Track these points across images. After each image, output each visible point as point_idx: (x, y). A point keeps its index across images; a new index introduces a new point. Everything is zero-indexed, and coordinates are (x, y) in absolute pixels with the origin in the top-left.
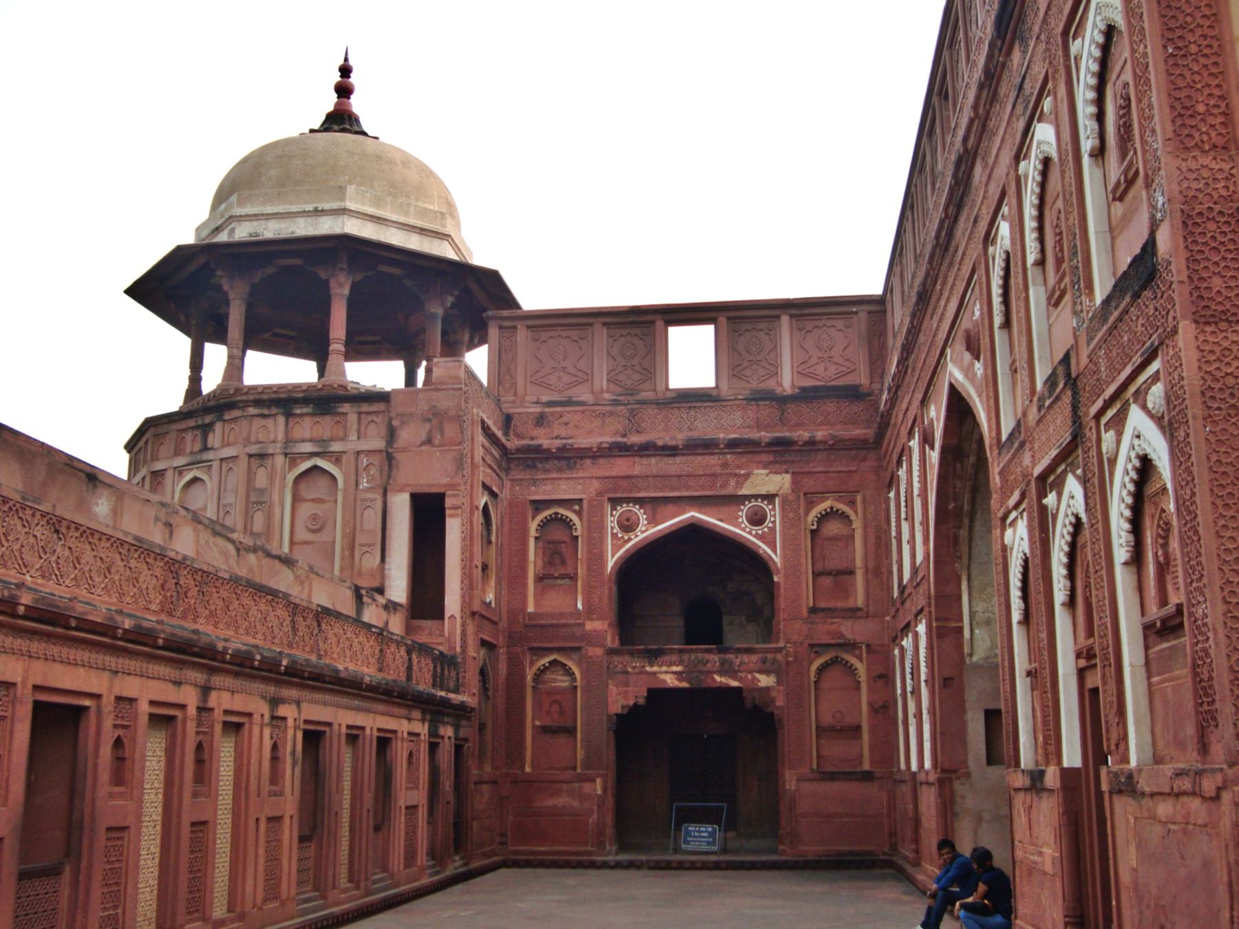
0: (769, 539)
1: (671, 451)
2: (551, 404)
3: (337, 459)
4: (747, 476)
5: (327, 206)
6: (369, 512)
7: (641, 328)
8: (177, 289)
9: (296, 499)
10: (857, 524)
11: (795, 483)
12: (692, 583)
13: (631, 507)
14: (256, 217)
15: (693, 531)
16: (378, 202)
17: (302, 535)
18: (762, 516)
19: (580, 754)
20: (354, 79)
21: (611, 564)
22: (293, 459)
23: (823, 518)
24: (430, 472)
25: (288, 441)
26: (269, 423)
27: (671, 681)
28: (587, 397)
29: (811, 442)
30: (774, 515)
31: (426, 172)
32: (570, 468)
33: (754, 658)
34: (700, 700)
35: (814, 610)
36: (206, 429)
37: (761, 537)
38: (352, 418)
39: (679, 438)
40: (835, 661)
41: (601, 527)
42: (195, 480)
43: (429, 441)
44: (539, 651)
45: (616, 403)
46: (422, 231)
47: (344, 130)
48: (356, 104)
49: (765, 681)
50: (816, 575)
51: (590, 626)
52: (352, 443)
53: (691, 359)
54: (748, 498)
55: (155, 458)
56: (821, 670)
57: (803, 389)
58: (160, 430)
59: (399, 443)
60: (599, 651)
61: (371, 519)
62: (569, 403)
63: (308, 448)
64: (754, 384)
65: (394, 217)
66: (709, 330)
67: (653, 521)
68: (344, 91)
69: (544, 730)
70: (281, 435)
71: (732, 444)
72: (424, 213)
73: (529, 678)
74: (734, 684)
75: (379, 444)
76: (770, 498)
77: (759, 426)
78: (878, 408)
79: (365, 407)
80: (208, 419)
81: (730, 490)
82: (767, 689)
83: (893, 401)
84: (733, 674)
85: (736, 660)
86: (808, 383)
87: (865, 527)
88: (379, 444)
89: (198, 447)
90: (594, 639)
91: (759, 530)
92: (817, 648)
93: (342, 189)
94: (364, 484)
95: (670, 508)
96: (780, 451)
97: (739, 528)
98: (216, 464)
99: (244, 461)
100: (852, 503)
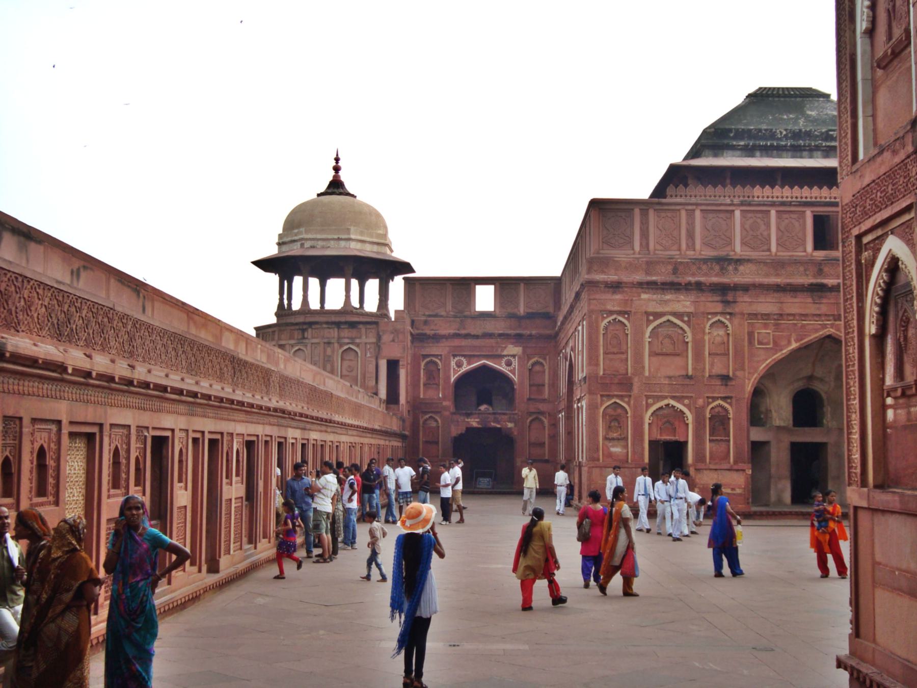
0: (513, 372)
1: (476, 337)
2: (430, 316)
3: (358, 345)
4: (505, 347)
5: (343, 237)
6: (370, 366)
7: (465, 286)
8: (280, 266)
9: (342, 359)
10: (546, 367)
11: (524, 352)
12: (484, 386)
13: (462, 359)
15: (484, 367)
16: (362, 233)
17: (345, 373)
18: (510, 363)
19: (440, 452)
20: (340, 164)
21: (452, 380)
22: (341, 345)
23: (533, 365)
24: (395, 352)
25: (339, 338)
26: (331, 330)
27: (475, 424)
28: (443, 313)
29: (530, 335)
30: (515, 363)
31: (378, 215)
32: (438, 342)
33: (506, 417)
34: (486, 431)
35: (529, 399)
36: (304, 331)
37: (510, 371)
38: (363, 330)
39: (479, 332)
40: (537, 418)
41: (450, 364)
42: (299, 349)
43: (393, 341)
44: (425, 413)
45: (455, 317)
46: (378, 244)
47: (340, 194)
48: (343, 176)
49: (510, 425)
50: (530, 386)
51: (445, 403)
52: (364, 339)
53: (485, 299)
54: (506, 356)
55: (279, 339)
56: (531, 422)
57: (528, 313)
58: (282, 328)
59: (383, 341)
60: (447, 413)
61: (372, 368)
62: (436, 316)
63: (346, 341)
64: (509, 310)
65: (368, 239)
66: (491, 288)
67: (469, 364)
68: (337, 169)
69: (427, 442)
70: (336, 335)
71: (500, 335)
72: (379, 236)
73: (421, 423)
74: (499, 426)
75: (374, 340)
76: (514, 356)
77: (511, 329)
78: (556, 323)
79: (368, 326)
80: (305, 327)
81: (499, 352)
82: (510, 428)
83: (560, 329)
84: (498, 422)
85: (500, 417)
86: (530, 311)
87: (550, 368)
88: (374, 340)
89: (300, 337)
90: (446, 408)
91: (509, 368)
92: (530, 414)
93: (348, 231)
94: (368, 355)
95: (475, 359)
96: (518, 339)
97: (502, 367)
98: (309, 346)
99: (322, 345)
100: (545, 359)
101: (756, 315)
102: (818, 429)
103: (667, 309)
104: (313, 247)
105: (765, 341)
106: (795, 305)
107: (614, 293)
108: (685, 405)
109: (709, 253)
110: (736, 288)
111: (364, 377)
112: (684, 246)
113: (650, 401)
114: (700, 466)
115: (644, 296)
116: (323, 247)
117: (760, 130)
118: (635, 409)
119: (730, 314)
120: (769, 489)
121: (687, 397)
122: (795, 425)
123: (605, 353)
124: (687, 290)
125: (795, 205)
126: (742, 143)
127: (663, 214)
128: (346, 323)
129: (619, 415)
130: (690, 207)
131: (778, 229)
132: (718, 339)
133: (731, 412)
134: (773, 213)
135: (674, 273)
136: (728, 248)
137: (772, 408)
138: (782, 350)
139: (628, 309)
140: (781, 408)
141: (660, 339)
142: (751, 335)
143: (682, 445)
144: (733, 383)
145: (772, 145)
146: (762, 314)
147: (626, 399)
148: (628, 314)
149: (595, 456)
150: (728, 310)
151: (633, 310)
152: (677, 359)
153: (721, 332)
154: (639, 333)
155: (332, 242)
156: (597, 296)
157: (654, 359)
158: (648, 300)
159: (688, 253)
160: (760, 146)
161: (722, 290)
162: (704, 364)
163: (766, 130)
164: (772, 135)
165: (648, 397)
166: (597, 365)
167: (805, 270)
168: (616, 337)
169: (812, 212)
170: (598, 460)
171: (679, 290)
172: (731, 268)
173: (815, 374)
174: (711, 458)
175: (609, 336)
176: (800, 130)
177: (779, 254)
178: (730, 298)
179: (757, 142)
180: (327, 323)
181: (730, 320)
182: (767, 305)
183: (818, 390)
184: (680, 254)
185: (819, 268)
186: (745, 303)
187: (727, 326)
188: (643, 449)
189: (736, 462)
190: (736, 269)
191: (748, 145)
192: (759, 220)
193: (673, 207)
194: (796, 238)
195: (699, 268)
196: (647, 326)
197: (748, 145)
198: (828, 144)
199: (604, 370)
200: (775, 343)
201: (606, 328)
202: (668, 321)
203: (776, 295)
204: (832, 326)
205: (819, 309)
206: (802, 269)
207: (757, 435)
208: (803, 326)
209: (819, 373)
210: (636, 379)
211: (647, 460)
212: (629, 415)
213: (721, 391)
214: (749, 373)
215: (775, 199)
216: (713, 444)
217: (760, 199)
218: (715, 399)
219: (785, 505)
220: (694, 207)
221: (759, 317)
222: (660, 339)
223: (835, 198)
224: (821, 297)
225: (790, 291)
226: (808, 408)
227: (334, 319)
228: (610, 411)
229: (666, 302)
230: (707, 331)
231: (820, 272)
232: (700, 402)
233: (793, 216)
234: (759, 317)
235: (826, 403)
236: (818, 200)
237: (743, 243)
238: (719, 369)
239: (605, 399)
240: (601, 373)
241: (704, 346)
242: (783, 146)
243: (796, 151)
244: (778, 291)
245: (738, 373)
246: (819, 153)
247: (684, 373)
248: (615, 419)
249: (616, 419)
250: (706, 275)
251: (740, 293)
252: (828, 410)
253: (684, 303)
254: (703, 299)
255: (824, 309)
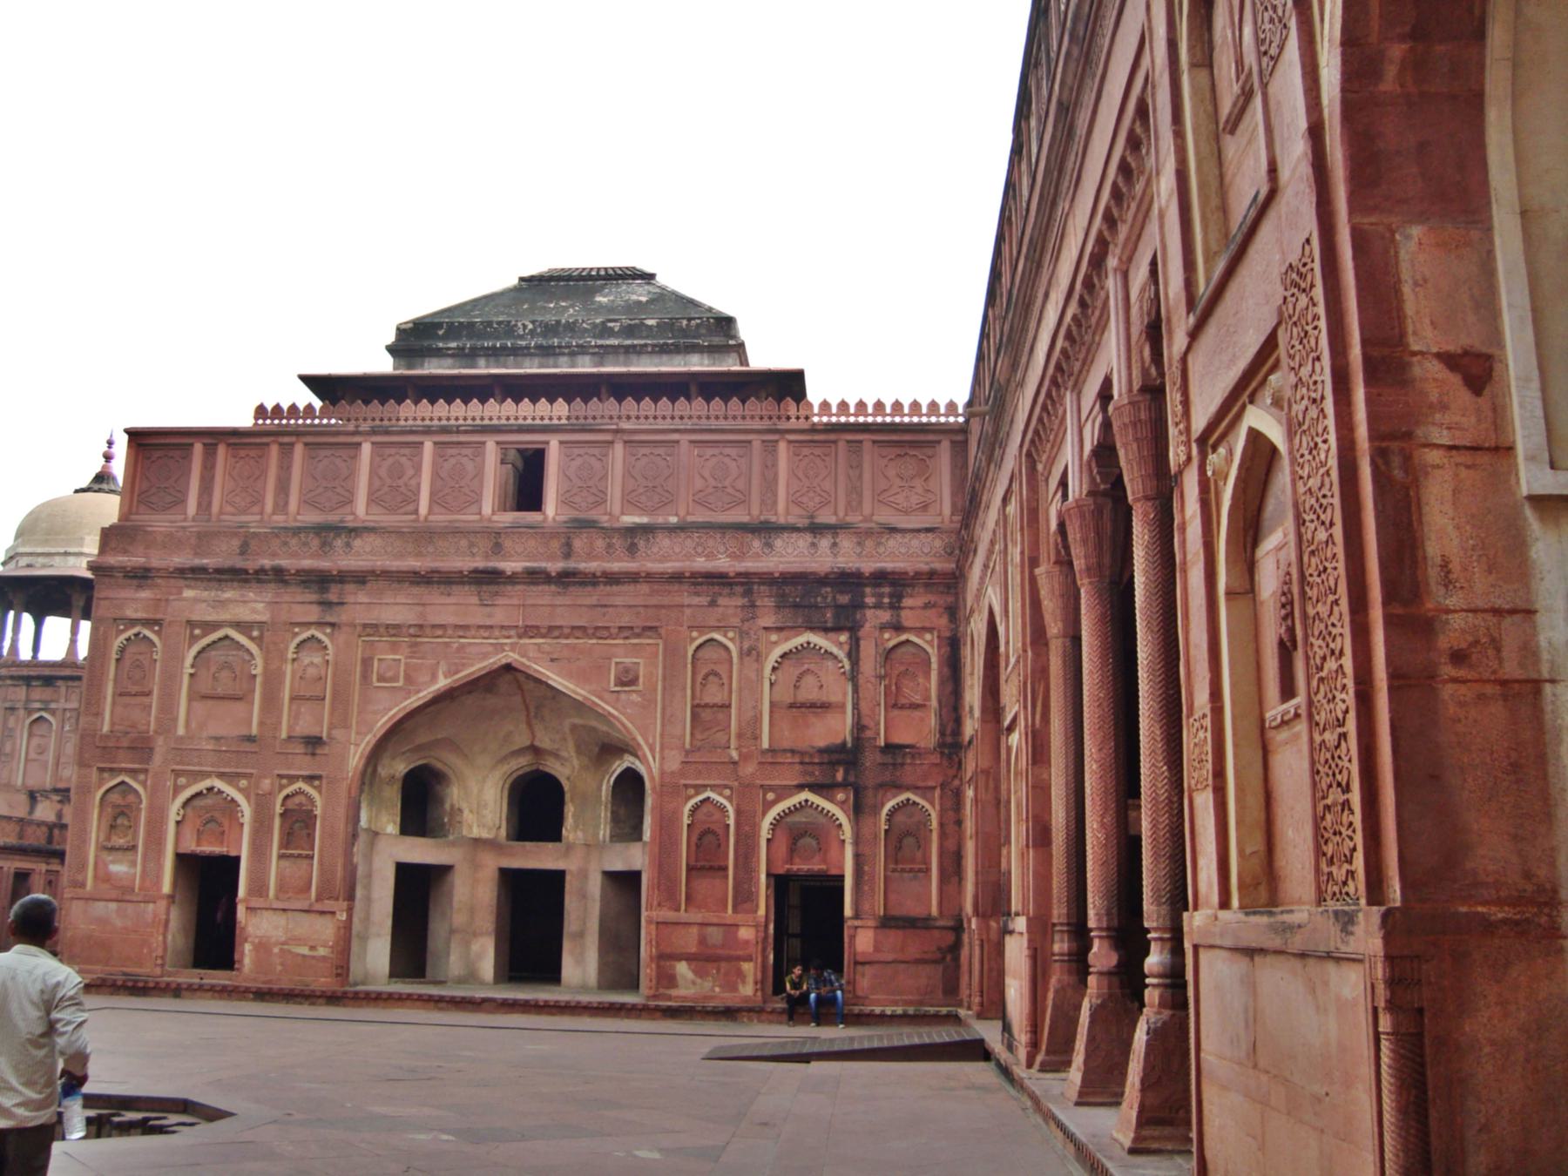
3: (53, 712)
9: (30, 735)
14: (31, 554)
22: (30, 712)
25: (28, 700)
38: (63, 690)
63: (37, 705)
70: (23, 697)
75: (75, 705)
93: (82, 539)
94: (67, 728)
101: (376, 626)
102: (550, 845)
103: (225, 616)
104: (29, 566)
105: (389, 674)
106: (448, 608)
107: (140, 587)
108: (240, 790)
109: (312, 517)
110: (343, 577)
111: (57, 764)
112: (269, 507)
113: (182, 781)
114: (256, 902)
115: (189, 593)
116: (44, 566)
117: (490, 324)
118: (153, 795)
119: (332, 625)
120: (448, 954)
121: (244, 776)
122: (509, 837)
123: (120, 694)
124: (259, 581)
125: (466, 432)
126: (453, 345)
127: (242, 453)
128: (38, 678)
129: (128, 806)
130: (286, 439)
131: (436, 475)
132: (311, 672)
133: (319, 803)
134: (428, 446)
135: (242, 553)
136: (347, 509)
137: (464, 806)
138: (418, 691)
139: (158, 616)
140: (480, 801)
141: (213, 669)
142: (367, 663)
143: (230, 865)
144: (326, 750)
145: (504, 348)
146: (388, 626)
147: (142, 777)
148: (160, 625)
149: (80, 878)
150: (329, 619)
151: (168, 618)
152: (239, 707)
153: (317, 660)
154: (174, 658)
155: (57, 559)
156: (111, 594)
157: (200, 707)
158: (195, 601)
159: (275, 518)
160: (483, 348)
161: (320, 581)
162: (280, 717)
163: (499, 323)
164: (509, 330)
165: (177, 773)
166: (99, 714)
167: (472, 545)
168: (138, 665)
169: (498, 443)
170: (83, 885)
171: (246, 581)
172: (339, 543)
173: (537, 743)
174: (281, 888)
175: (127, 663)
176: (558, 322)
177: (431, 518)
178: (333, 597)
179: (479, 343)
180: (12, 678)
181: (330, 636)
182: (397, 608)
183: (553, 772)
184: (261, 521)
185: (496, 539)
186: (360, 606)
187: (326, 648)
188: (160, 868)
189: (319, 899)
190: (348, 545)
191: (463, 349)
192: (403, 460)
193: (258, 440)
194: (466, 490)
195: (285, 543)
196: (190, 646)
197: (463, 349)
198: (600, 342)
199: (113, 724)
200: (408, 679)
201: (122, 650)
202: (227, 637)
203: (416, 590)
204: (513, 647)
205: (490, 616)
206: (464, 543)
207: (420, 851)
208: (462, 647)
209: (544, 742)
210: (160, 741)
211: (166, 887)
212: (143, 806)
213: (304, 766)
214: (358, 733)
215: (427, 422)
216: (285, 863)
217: (410, 422)
218: (292, 779)
219: (482, 983)
220: (293, 439)
221: (382, 630)
222: (213, 669)
223: (542, 418)
224: (497, 594)
225: (439, 583)
226: (537, 807)
227: (47, 672)
228: (115, 797)
229: (223, 603)
230: (290, 656)
231: (497, 549)
232: (266, 784)
233: (468, 451)
234: (382, 630)
235: (567, 797)
236: (512, 421)
237: (372, 499)
238: (305, 727)
239: (106, 775)
240: (106, 728)
241: (282, 682)
242: (522, 348)
243: (547, 352)
244: (418, 583)
245: (334, 732)
246: (587, 358)
247: (245, 732)
248: (120, 814)
249: (122, 813)
250: (294, 555)
251: (350, 587)
252: (570, 810)
253: (253, 605)
254: (287, 598)
255: (499, 616)
